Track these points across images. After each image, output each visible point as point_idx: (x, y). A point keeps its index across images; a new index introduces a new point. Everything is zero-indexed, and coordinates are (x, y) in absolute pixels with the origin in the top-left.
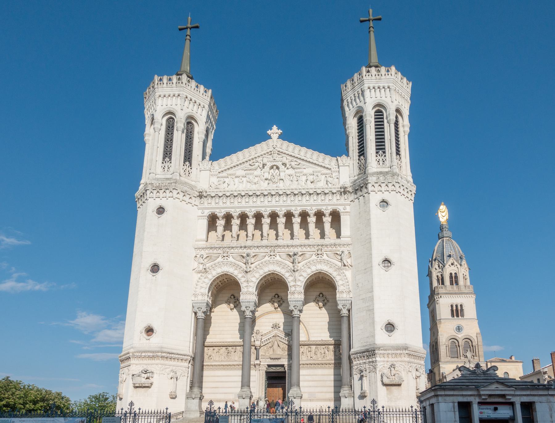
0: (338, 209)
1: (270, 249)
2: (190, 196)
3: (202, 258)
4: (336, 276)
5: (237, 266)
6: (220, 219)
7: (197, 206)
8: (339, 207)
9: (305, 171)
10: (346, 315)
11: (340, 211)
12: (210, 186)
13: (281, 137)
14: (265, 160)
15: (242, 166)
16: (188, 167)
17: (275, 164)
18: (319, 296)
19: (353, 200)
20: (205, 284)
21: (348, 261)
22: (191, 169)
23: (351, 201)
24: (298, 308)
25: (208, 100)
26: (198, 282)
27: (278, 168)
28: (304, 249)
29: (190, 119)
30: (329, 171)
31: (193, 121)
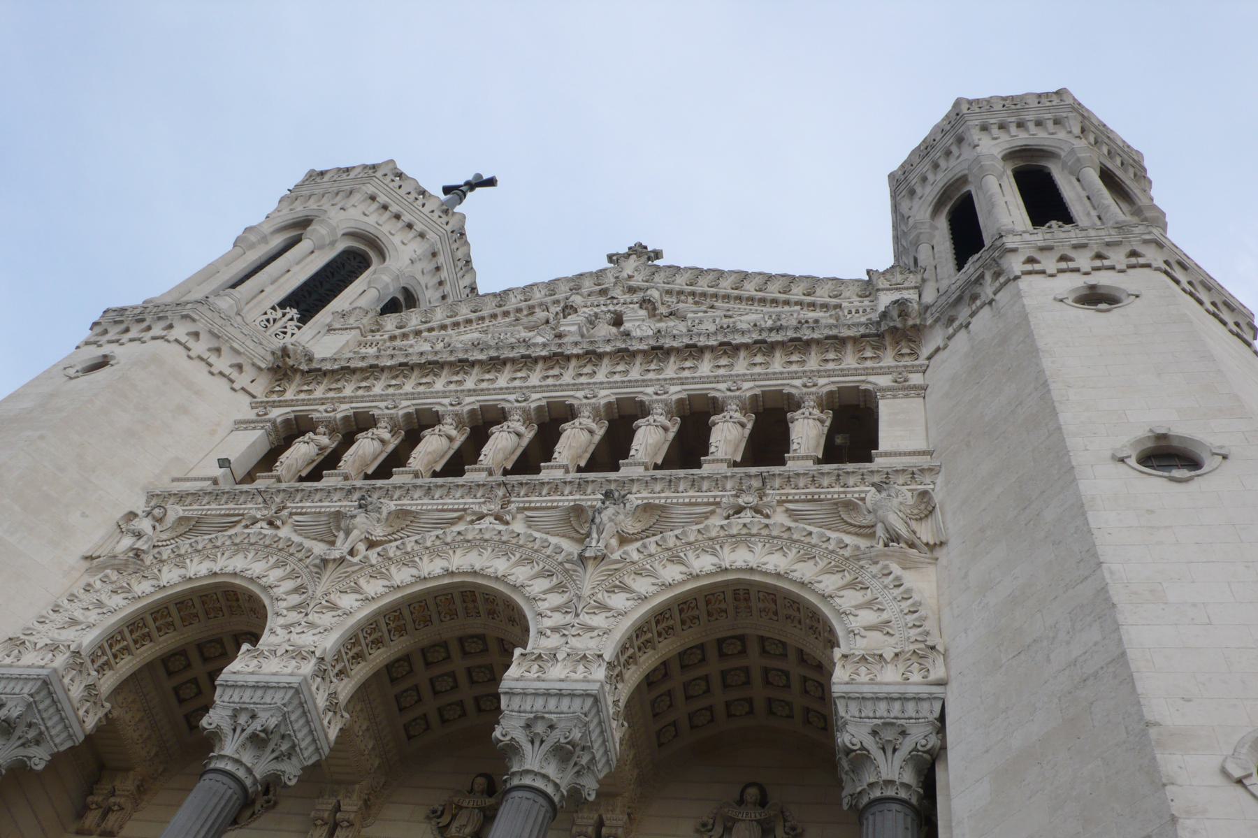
6: (321, 429)
7: (254, 397)
10: (903, 794)
16: (292, 319)
18: (741, 802)
19: (938, 350)
22: (299, 328)
23: (929, 358)
24: (556, 736)
26: (72, 598)
29: (369, 246)
31: (372, 254)
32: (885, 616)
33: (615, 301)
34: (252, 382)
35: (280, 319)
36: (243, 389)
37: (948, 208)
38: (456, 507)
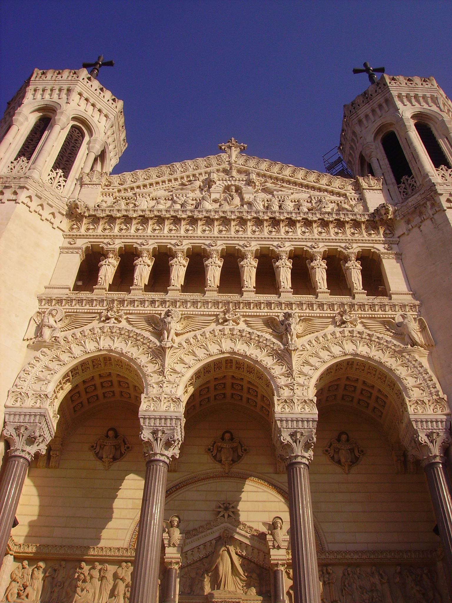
0: (375, 248)
1: (224, 308)
2: (52, 210)
3: (53, 316)
4: (396, 366)
5: (137, 340)
6: (111, 255)
8: (376, 246)
9: (296, 196)
11: (378, 252)
12: (98, 206)
13: (242, 151)
14: (214, 176)
15: (167, 185)
16: (60, 177)
17: (233, 183)
19: (404, 234)
20: (51, 372)
21: (418, 337)
22: (65, 181)
23: (399, 237)
25: (115, 109)
27: (238, 190)
28: (308, 311)
30: (342, 198)
32: (418, 382)
33: (234, 179)
34: (61, 222)
35: (56, 177)
36: (58, 227)
37: (381, 136)
38: (210, 313)
